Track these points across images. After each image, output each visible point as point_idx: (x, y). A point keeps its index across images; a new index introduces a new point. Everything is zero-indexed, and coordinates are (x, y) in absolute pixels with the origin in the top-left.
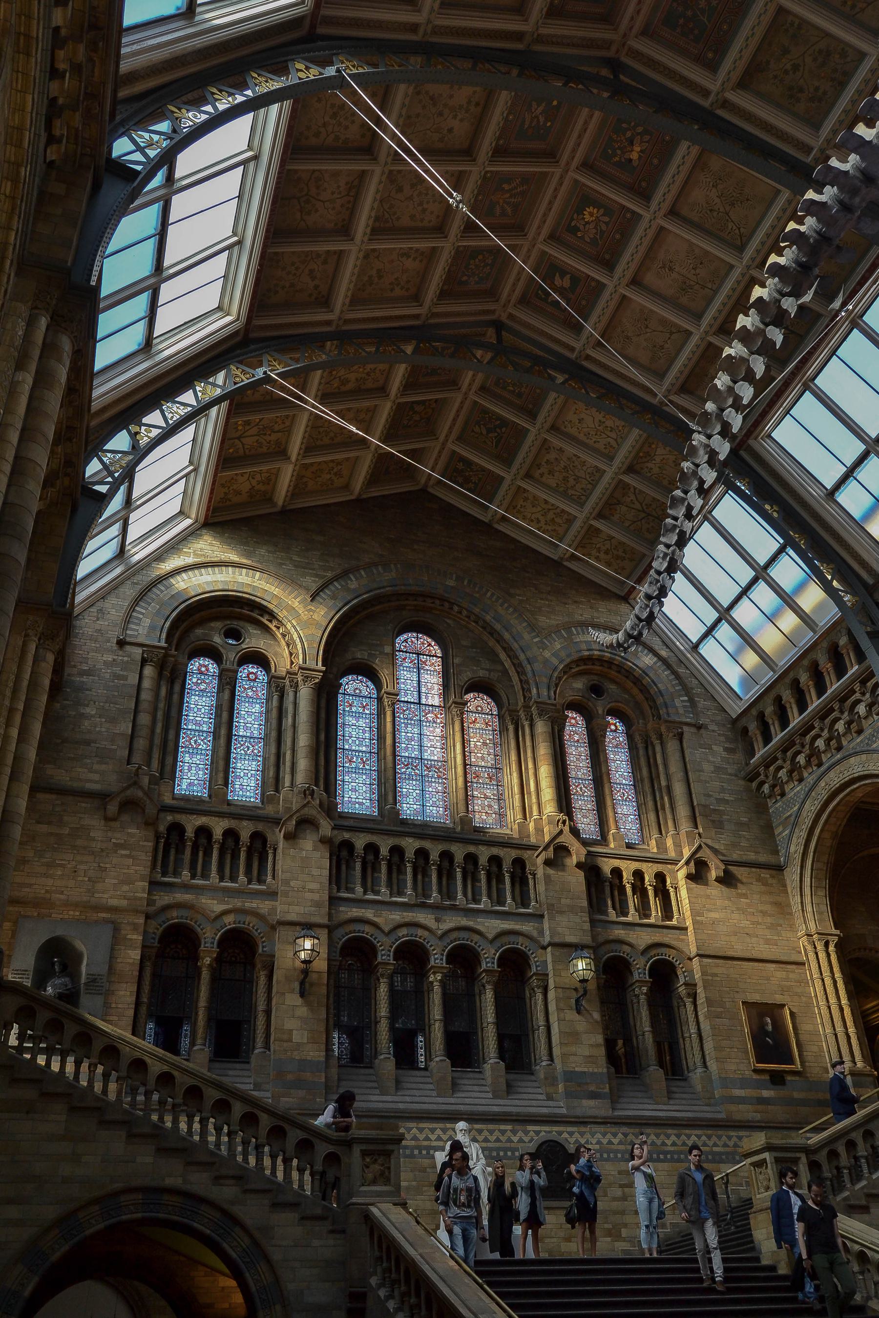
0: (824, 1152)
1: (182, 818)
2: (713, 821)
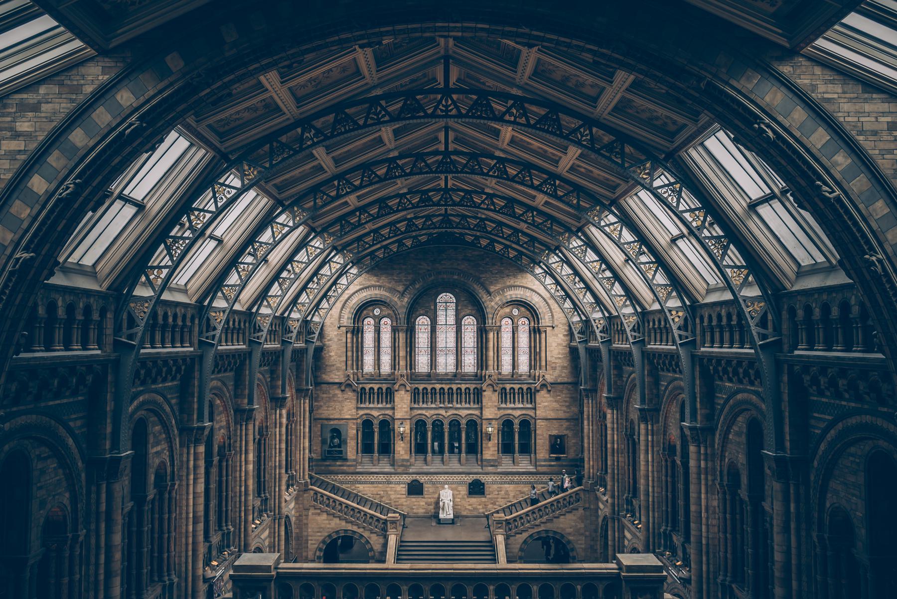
1: (364, 386)
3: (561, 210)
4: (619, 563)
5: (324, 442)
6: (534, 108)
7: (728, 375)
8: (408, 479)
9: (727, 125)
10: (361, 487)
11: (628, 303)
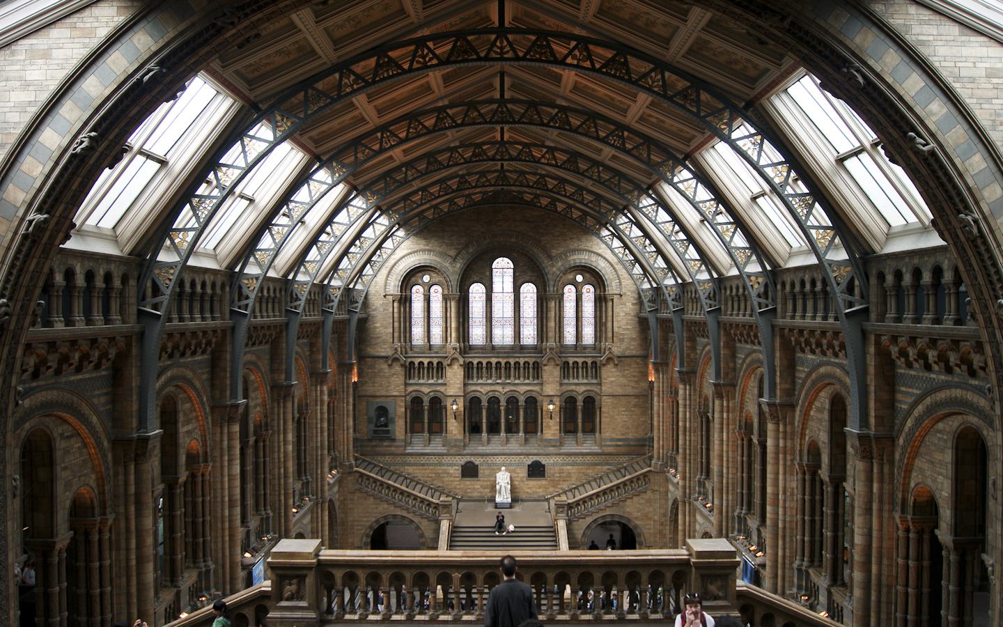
1: (413, 360)
3: (629, 166)
4: (689, 548)
5: (370, 421)
6: (599, 50)
7: (811, 346)
8: (463, 460)
9: (813, 69)
10: (410, 469)
11: (703, 268)
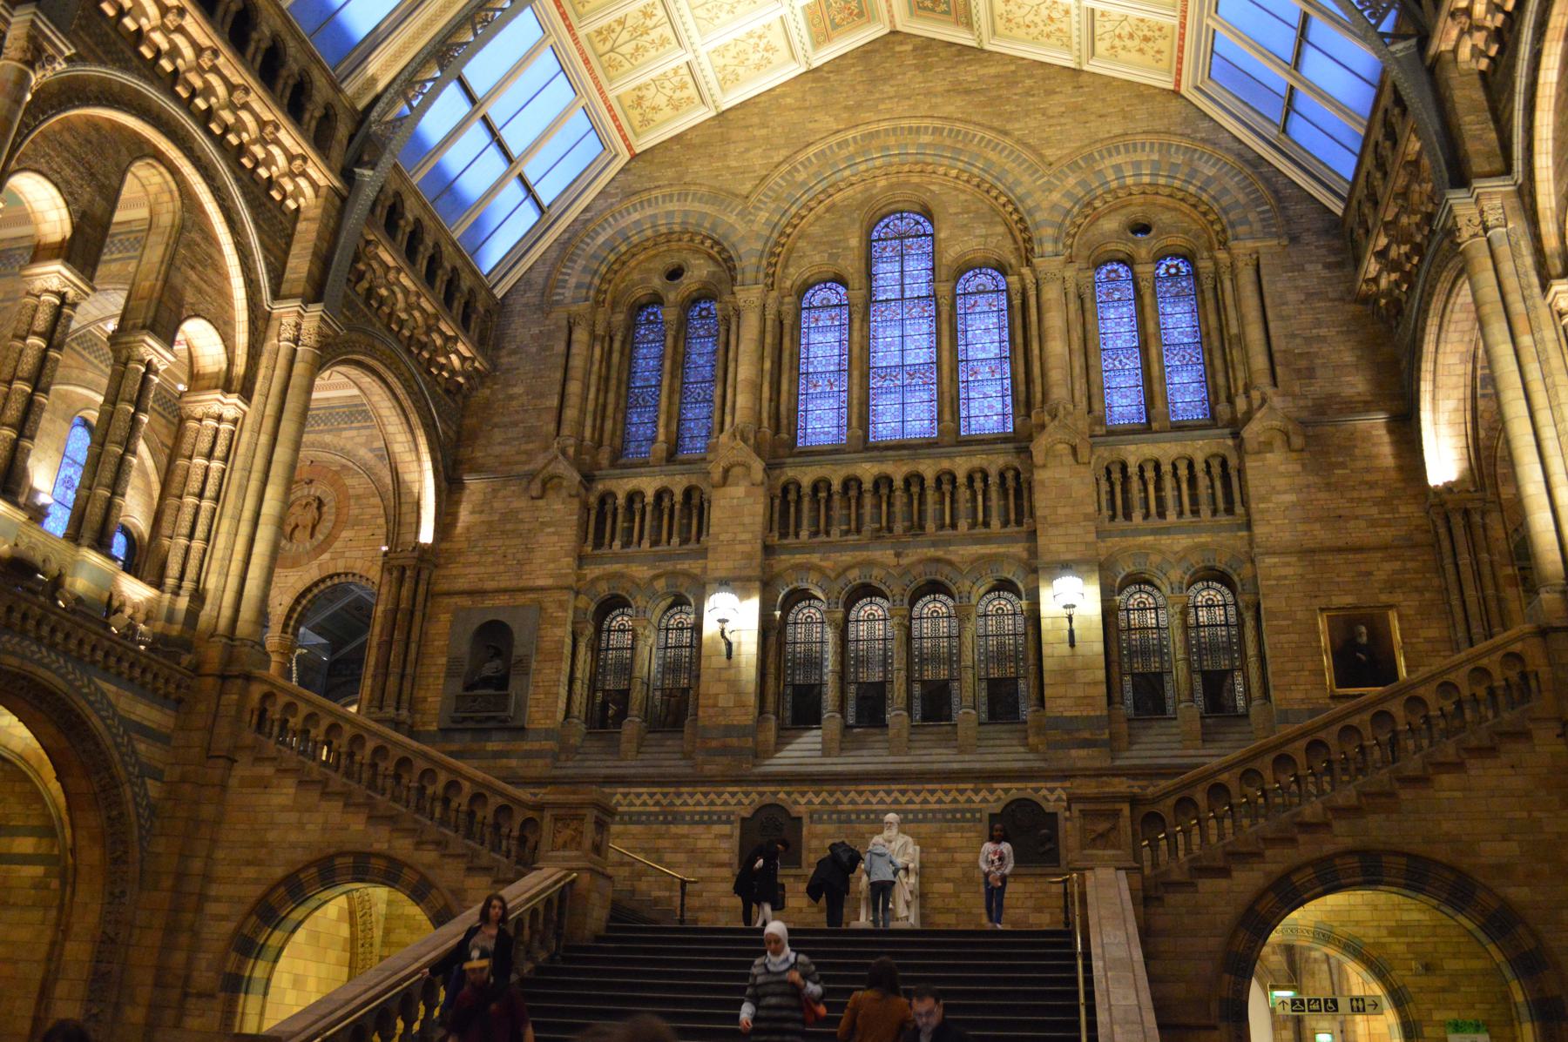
0: (1171, 801)
1: (611, 485)
2: (1299, 371)
5: (451, 673)
